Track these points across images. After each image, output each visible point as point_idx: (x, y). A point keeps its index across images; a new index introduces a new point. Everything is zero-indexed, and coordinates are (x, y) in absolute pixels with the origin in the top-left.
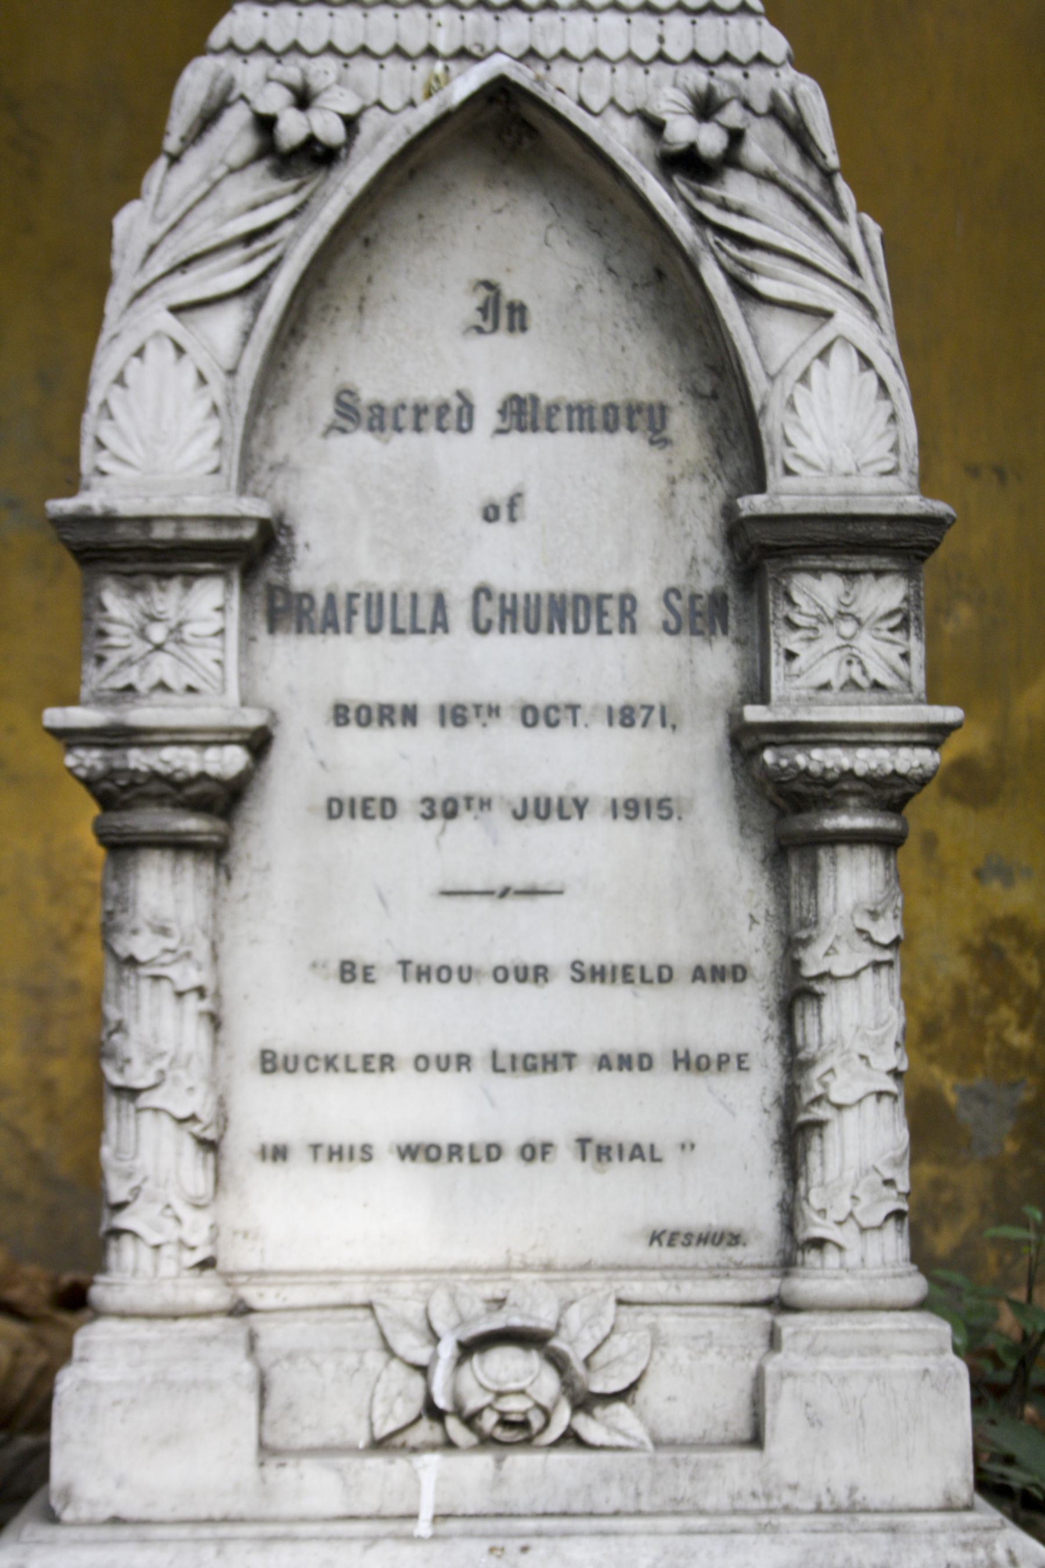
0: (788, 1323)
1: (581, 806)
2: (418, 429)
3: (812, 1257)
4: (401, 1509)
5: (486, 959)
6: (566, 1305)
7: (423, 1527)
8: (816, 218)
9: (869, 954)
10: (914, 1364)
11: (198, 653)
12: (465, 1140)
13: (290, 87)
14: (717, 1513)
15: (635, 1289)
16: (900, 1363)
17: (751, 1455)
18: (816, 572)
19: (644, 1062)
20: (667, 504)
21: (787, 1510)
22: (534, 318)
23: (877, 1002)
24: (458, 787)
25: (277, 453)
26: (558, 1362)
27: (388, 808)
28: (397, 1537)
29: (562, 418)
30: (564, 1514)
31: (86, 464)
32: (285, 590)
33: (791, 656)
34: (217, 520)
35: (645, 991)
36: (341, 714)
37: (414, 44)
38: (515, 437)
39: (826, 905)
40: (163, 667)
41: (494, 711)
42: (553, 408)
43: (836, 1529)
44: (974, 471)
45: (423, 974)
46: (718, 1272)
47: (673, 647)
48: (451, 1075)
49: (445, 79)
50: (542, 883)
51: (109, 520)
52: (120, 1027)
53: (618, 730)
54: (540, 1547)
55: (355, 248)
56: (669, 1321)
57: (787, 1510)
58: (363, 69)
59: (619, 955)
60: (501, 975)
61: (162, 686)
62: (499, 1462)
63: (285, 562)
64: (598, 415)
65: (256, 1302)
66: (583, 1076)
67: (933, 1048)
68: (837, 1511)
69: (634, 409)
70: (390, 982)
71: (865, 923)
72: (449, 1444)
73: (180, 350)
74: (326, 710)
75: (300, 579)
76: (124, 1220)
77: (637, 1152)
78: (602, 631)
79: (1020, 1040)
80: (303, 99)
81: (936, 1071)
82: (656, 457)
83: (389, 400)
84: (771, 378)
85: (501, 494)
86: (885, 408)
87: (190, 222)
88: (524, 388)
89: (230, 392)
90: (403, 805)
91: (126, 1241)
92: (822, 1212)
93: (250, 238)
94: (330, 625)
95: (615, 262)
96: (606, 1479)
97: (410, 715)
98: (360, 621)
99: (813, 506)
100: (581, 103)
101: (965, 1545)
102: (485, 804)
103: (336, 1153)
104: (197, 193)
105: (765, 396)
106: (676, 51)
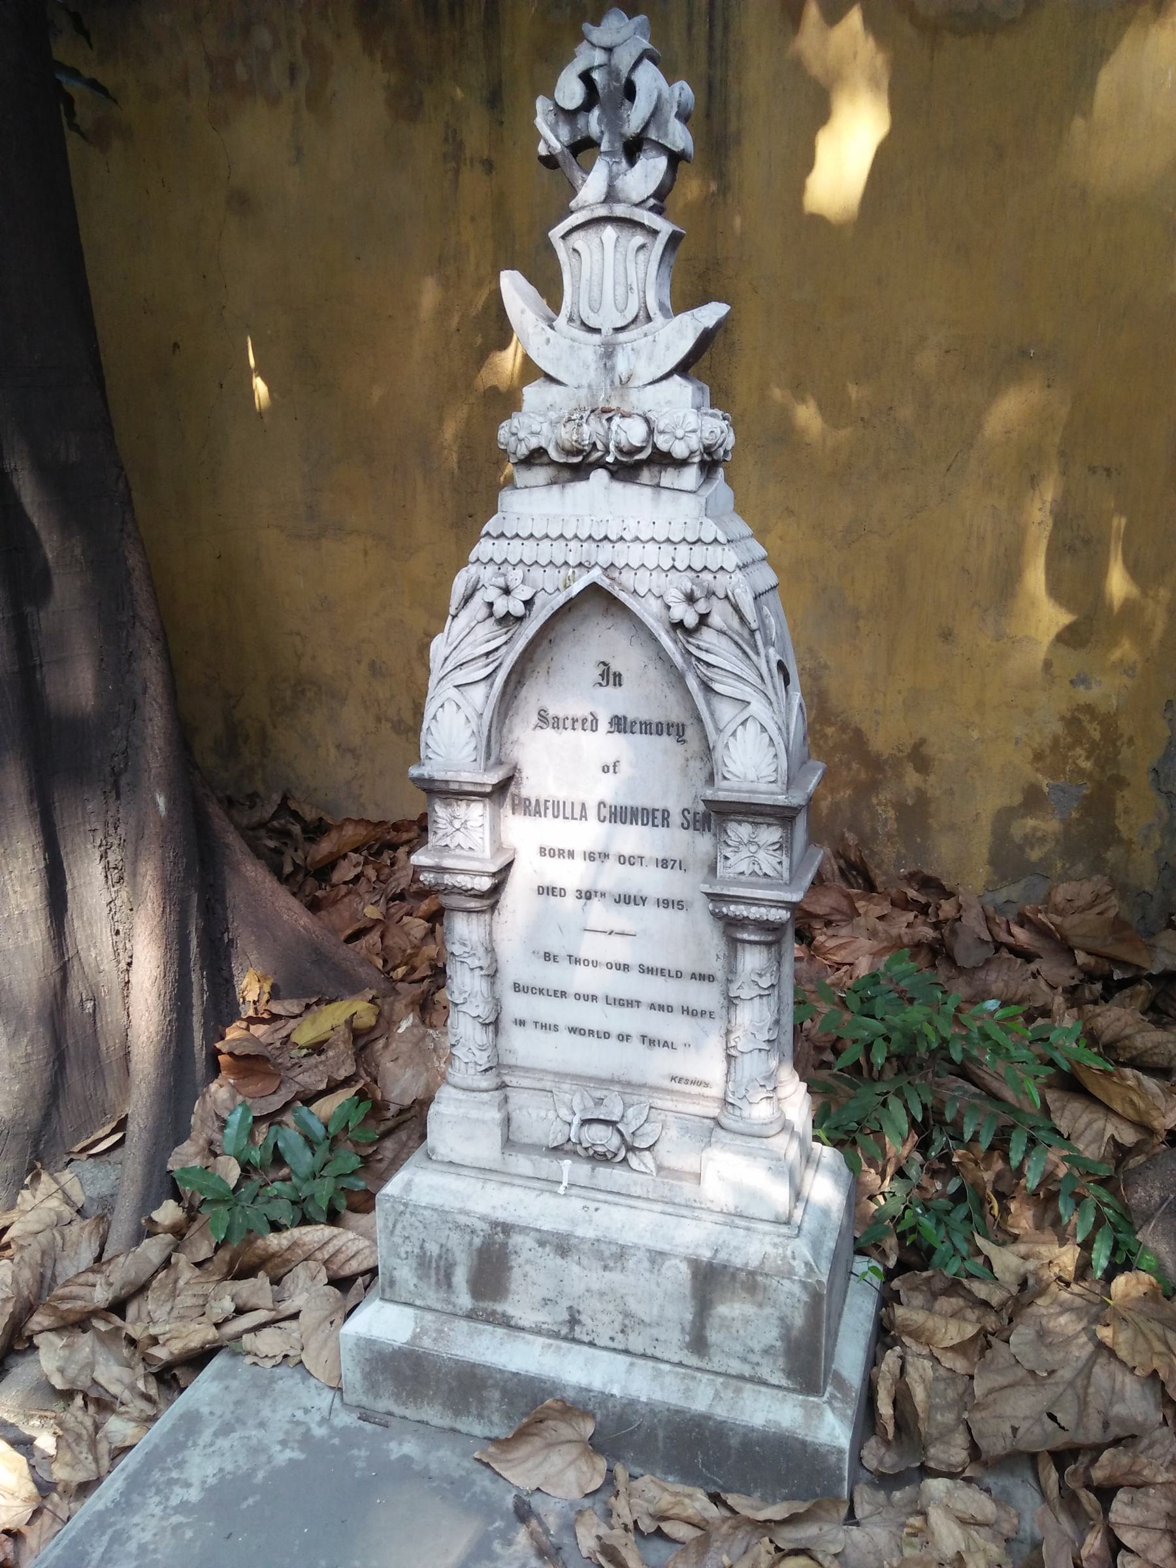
1: (644, 900)
6: (626, 1106)
7: (561, 1190)
8: (744, 652)
9: (756, 991)
11: (473, 834)
12: (595, 1029)
13: (500, 588)
18: (740, 822)
19: (670, 1009)
23: (761, 1011)
25: (514, 736)
28: (551, 1192)
31: (422, 755)
32: (518, 796)
33: (726, 858)
35: (670, 980)
37: (559, 561)
39: (740, 967)
40: (459, 838)
42: (633, 723)
44: (1093, 470)
47: (686, 835)
48: (589, 1003)
51: (431, 780)
55: (545, 643)
58: (537, 572)
59: (659, 963)
63: (518, 784)
64: (654, 727)
66: (643, 1011)
67: (1040, 765)
71: (756, 978)
75: (525, 793)
77: (666, 1044)
78: (654, 825)
79: (1087, 765)
80: (507, 591)
81: (1040, 776)
82: (680, 748)
83: (561, 715)
86: (772, 751)
87: (463, 645)
89: (480, 726)
93: (488, 654)
94: (537, 813)
96: (635, 1183)
98: (550, 812)
99: (734, 797)
101: (775, 1245)
102: (603, 895)
103: (544, 1027)
104: (465, 633)
105: (715, 742)
106: (681, 566)
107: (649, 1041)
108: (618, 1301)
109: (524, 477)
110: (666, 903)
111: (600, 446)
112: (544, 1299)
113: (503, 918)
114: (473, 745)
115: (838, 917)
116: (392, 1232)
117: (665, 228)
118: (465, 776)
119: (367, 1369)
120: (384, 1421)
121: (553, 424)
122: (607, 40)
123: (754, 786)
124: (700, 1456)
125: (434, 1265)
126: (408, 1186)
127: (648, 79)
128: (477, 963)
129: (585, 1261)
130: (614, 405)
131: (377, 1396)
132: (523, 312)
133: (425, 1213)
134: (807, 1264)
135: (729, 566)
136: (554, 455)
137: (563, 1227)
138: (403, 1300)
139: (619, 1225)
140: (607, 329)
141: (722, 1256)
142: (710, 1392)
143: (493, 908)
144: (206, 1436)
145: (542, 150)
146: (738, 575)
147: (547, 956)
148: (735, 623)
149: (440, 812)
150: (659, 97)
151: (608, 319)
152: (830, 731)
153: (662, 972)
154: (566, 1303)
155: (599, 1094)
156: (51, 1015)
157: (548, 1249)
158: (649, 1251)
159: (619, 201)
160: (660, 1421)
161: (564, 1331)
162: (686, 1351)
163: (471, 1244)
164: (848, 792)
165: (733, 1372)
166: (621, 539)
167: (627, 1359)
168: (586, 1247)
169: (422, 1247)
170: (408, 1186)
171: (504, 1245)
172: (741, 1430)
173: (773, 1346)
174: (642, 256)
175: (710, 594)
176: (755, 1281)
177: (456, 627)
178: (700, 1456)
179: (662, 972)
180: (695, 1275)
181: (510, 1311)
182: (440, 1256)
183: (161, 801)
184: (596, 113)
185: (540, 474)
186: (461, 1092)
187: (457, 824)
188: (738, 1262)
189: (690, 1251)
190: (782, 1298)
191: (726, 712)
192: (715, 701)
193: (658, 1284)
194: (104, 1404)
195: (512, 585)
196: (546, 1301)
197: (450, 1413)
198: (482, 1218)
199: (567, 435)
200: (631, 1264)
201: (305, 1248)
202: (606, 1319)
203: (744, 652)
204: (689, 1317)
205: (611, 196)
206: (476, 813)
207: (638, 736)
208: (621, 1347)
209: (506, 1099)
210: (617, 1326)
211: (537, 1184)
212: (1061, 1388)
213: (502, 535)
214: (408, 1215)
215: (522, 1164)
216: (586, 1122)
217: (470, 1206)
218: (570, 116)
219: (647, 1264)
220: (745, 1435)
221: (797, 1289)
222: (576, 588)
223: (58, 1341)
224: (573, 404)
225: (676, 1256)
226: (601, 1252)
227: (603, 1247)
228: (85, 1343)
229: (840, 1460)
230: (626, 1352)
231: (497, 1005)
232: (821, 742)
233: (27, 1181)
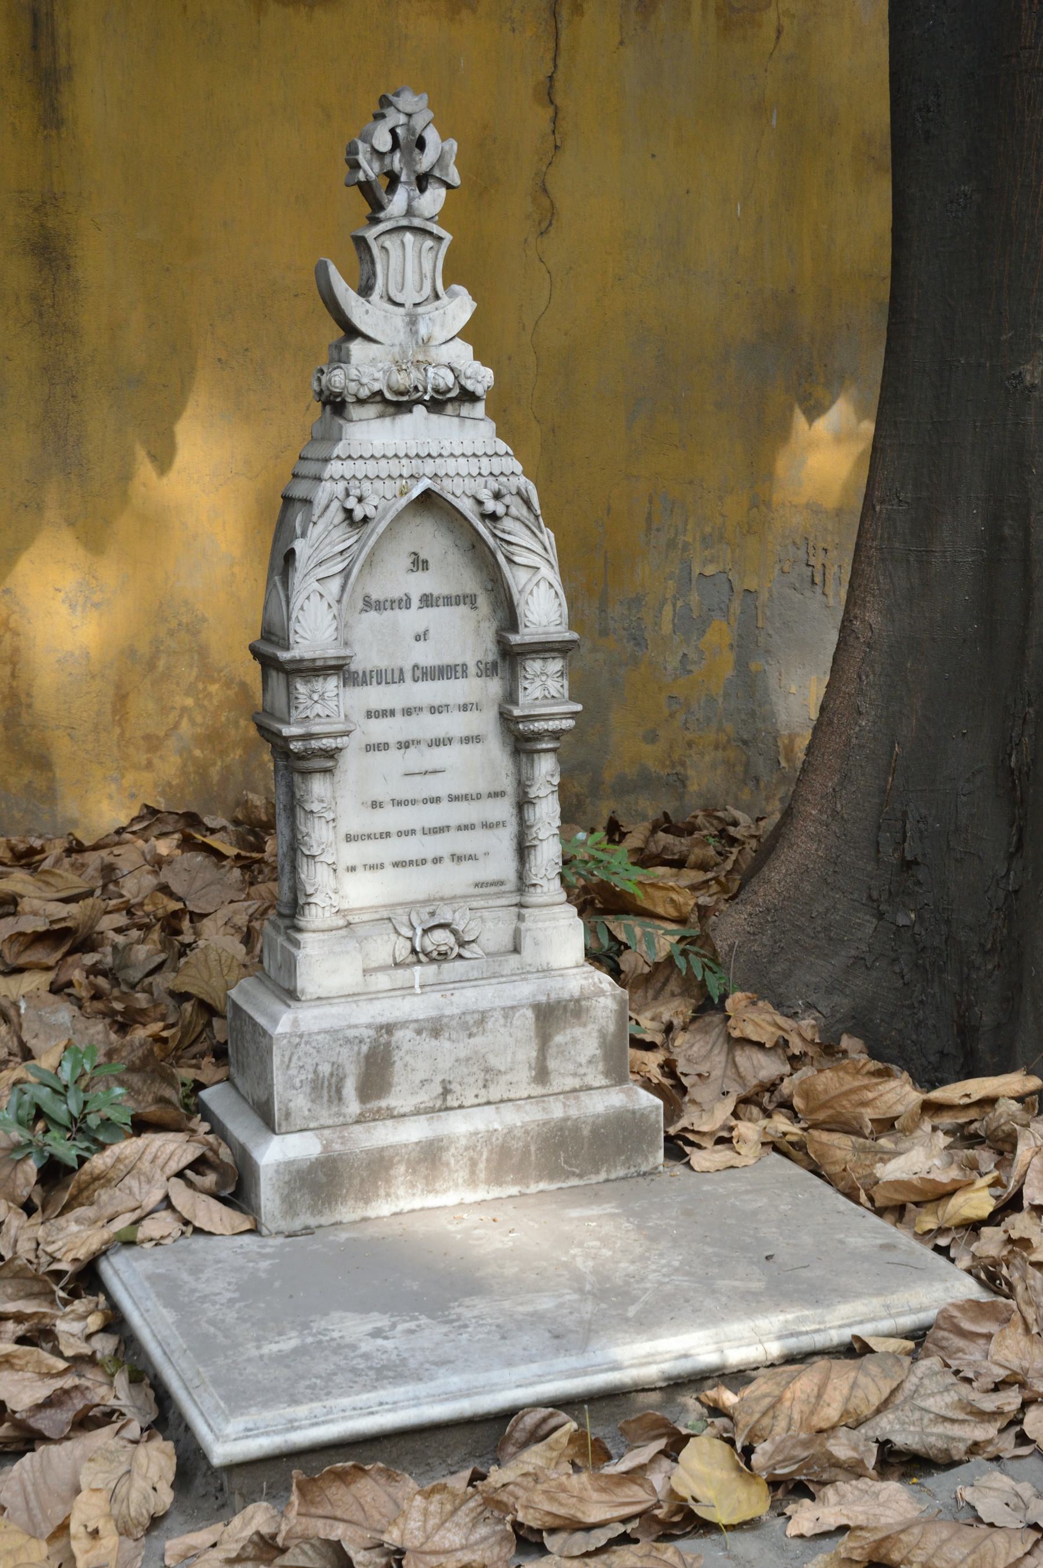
0: (524, 911)
1: (450, 740)
2: (392, 609)
3: (532, 889)
4: (409, 985)
5: (419, 797)
8: (533, 532)
11: (330, 703)
14: (507, 976)
15: (474, 904)
16: (562, 922)
17: (516, 956)
18: (533, 659)
20: (477, 630)
21: (528, 972)
22: (431, 565)
24: (410, 737)
26: (454, 932)
27: (386, 746)
28: (410, 994)
29: (441, 602)
30: (460, 981)
33: (525, 689)
35: (473, 803)
36: (369, 714)
38: (425, 609)
39: (537, 773)
40: (318, 709)
41: (421, 709)
43: (545, 977)
45: (399, 803)
48: (409, 837)
50: (438, 768)
51: (302, 660)
52: (307, 834)
53: (462, 713)
54: (457, 993)
56: (486, 914)
57: (528, 972)
60: (425, 801)
61: (318, 715)
62: (439, 967)
64: (453, 599)
65: (352, 921)
66: (452, 834)
68: (544, 971)
69: (465, 597)
70: (389, 807)
71: (549, 778)
72: (419, 962)
73: (321, 596)
74: (364, 713)
76: (312, 900)
77: (472, 857)
78: (456, 678)
82: (473, 613)
83: (382, 599)
84: (520, 592)
85: (421, 631)
88: (428, 591)
90: (391, 745)
91: (312, 906)
92: (536, 875)
93: (341, 553)
94: (364, 682)
95: (458, 542)
96: (473, 969)
97: (392, 713)
98: (374, 680)
100: (453, 494)
102: (419, 742)
103: (372, 867)
106: (485, 472)
107: (456, 858)
108: (481, 1061)
109: (355, 412)
110: (467, 740)
111: (421, 388)
112: (421, 1082)
114: (334, 626)
116: (288, 1067)
119: (286, 1192)
122: (409, 110)
123: (546, 629)
124: (562, 1155)
125: (326, 1084)
127: (432, 136)
129: (454, 1036)
130: (420, 358)
132: (347, 290)
133: (318, 1037)
136: (388, 396)
137: (434, 1013)
138: (298, 1128)
139: (474, 1000)
140: (409, 304)
141: (553, 996)
142: (560, 1105)
147: (375, 805)
151: (409, 297)
152: (214, 688)
153: (466, 797)
154: (438, 1079)
155: (430, 909)
157: (424, 1035)
158: (503, 1009)
159: (414, 216)
160: (532, 1137)
161: (439, 1103)
162: (533, 1085)
163: (359, 1053)
164: (239, 752)
165: (567, 1088)
166: (441, 455)
167: (493, 1107)
168: (454, 1023)
169: (315, 1072)
171: (388, 1044)
172: (590, 1120)
173: (594, 1056)
176: (580, 1006)
178: (562, 1155)
179: (466, 797)
180: (537, 1018)
182: (332, 1075)
184: (397, 155)
185: (371, 410)
186: (321, 934)
188: (566, 996)
189: (531, 1000)
190: (599, 1013)
193: (511, 1035)
195: (365, 494)
196: (423, 1082)
197: (361, 1204)
198: (368, 1026)
200: (490, 1025)
201: (127, 1162)
202: (472, 1080)
203: (533, 532)
204: (534, 1054)
205: (410, 212)
207: (441, 608)
210: (481, 1083)
211: (398, 993)
212: (720, 1081)
214: (303, 1045)
217: (354, 1021)
219: (502, 1021)
220: (593, 1123)
225: (523, 1006)
226: (467, 1022)
227: (468, 1018)
229: (658, 1115)
230: (488, 1103)
232: (206, 703)
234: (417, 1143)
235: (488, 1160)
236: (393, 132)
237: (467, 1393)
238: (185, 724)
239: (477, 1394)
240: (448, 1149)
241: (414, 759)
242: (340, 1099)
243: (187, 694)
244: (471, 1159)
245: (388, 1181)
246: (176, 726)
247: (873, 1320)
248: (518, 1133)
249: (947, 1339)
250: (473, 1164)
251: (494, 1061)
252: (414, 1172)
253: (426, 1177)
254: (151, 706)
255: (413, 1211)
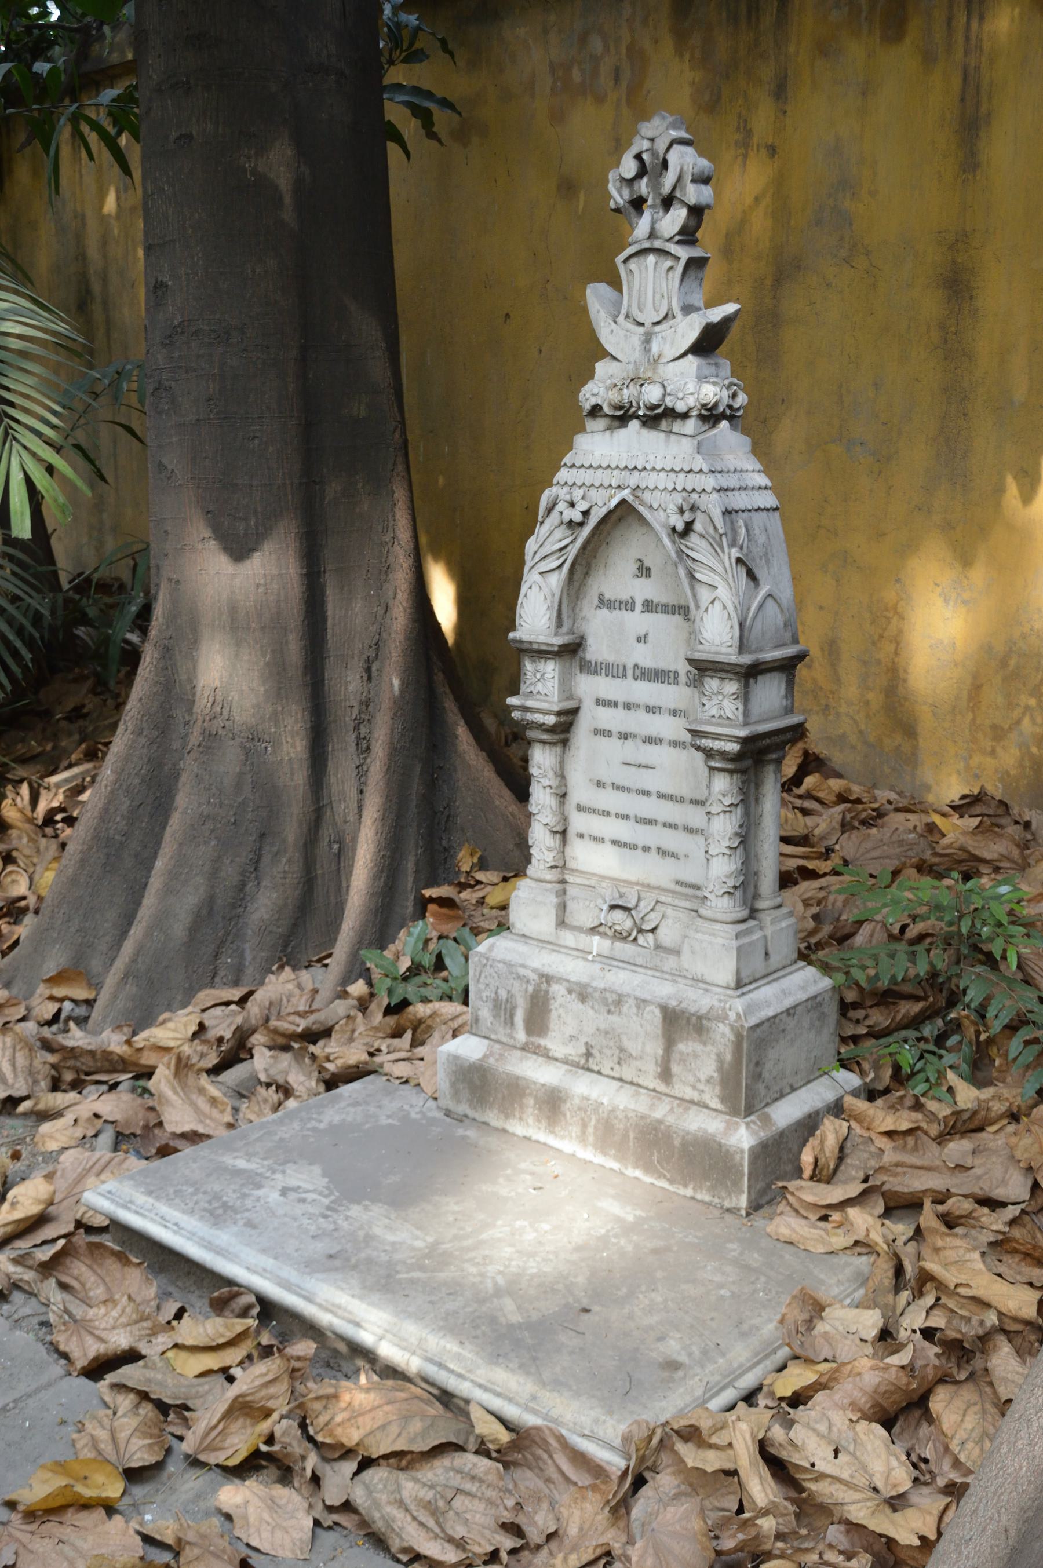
1: (661, 741)
5: (635, 787)
7: (590, 957)
10: (720, 941)
15: (663, 899)
18: (712, 677)
24: (628, 730)
25: (583, 614)
34: (547, 644)
36: (598, 702)
40: (540, 687)
41: (638, 706)
45: (618, 788)
46: (687, 897)
49: (612, 497)
50: (650, 764)
51: (521, 642)
56: (669, 911)
58: (593, 492)
63: (584, 650)
66: (659, 828)
69: (680, 607)
77: (673, 855)
80: (572, 505)
85: (642, 634)
88: (649, 598)
93: (561, 550)
94: (596, 672)
97: (616, 704)
107: (663, 853)
109: (591, 424)
113: (572, 753)
115: (1008, 865)
117: (684, 253)
118: (542, 639)
120: (462, 1119)
121: (607, 389)
123: (718, 649)
126: (491, 948)
128: (547, 783)
129: (596, 1007)
131: (459, 1101)
134: (738, 1014)
135: (709, 490)
136: (606, 409)
137: (585, 980)
140: (648, 324)
141: (683, 1005)
142: (668, 1108)
143: (565, 743)
144: (342, 1104)
145: (612, 205)
146: (715, 495)
147: (600, 784)
148: (711, 530)
149: (528, 666)
150: (681, 170)
151: (649, 316)
154: (583, 1039)
156: (305, 844)
158: (636, 999)
159: (657, 238)
165: (687, 1097)
167: (620, 1084)
168: (597, 995)
170: (491, 948)
171: (547, 992)
172: (681, 1133)
174: (671, 274)
175: (693, 508)
177: (542, 531)
181: (550, 1045)
183: (396, 683)
184: (645, 180)
185: (600, 423)
187: (538, 676)
188: (692, 1009)
190: (718, 1037)
191: (704, 595)
192: (698, 587)
194: (287, 1091)
197: (502, 1116)
198: (534, 971)
199: (614, 396)
200: (625, 1009)
202: (608, 1052)
204: (660, 1052)
205: (652, 235)
206: (550, 668)
207: (660, 615)
208: (617, 1075)
209: (564, 892)
210: (616, 1059)
211: (575, 953)
213: (573, 466)
215: (568, 938)
216: (613, 907)
218: (630, 182)
219: (634, 1010)
221: (727, 1030)
222: (614, 503)
223: (268, 1053)
224: (625, 375)
226: (606, 999)
227: (608, 995)
228: (286, 1058)
229: (742, 1158)
230: (621, 1080)
231: (565, 819)
233: (274, 968)
234: (543, 1085)
235: (595, 1127)
236: (638, 157)
237: (219, 1251)
238: (1026, 721)
239: (223, 1256)
240: (565, 1102)
241: (631, 750)
242: (512, 1024)
243: (1031, 695)
244: (582, 1119)
245: (522, 1107)
246: (1018, 722)
247: (510, 1400)
248: (621, 1115)
249: (545, 1463)
250: (584, 1126)
251: (627, 1044)
252: (540, 1109)
253: (549, 1118)
254: (1000, 700)
255: (538, 1142)
